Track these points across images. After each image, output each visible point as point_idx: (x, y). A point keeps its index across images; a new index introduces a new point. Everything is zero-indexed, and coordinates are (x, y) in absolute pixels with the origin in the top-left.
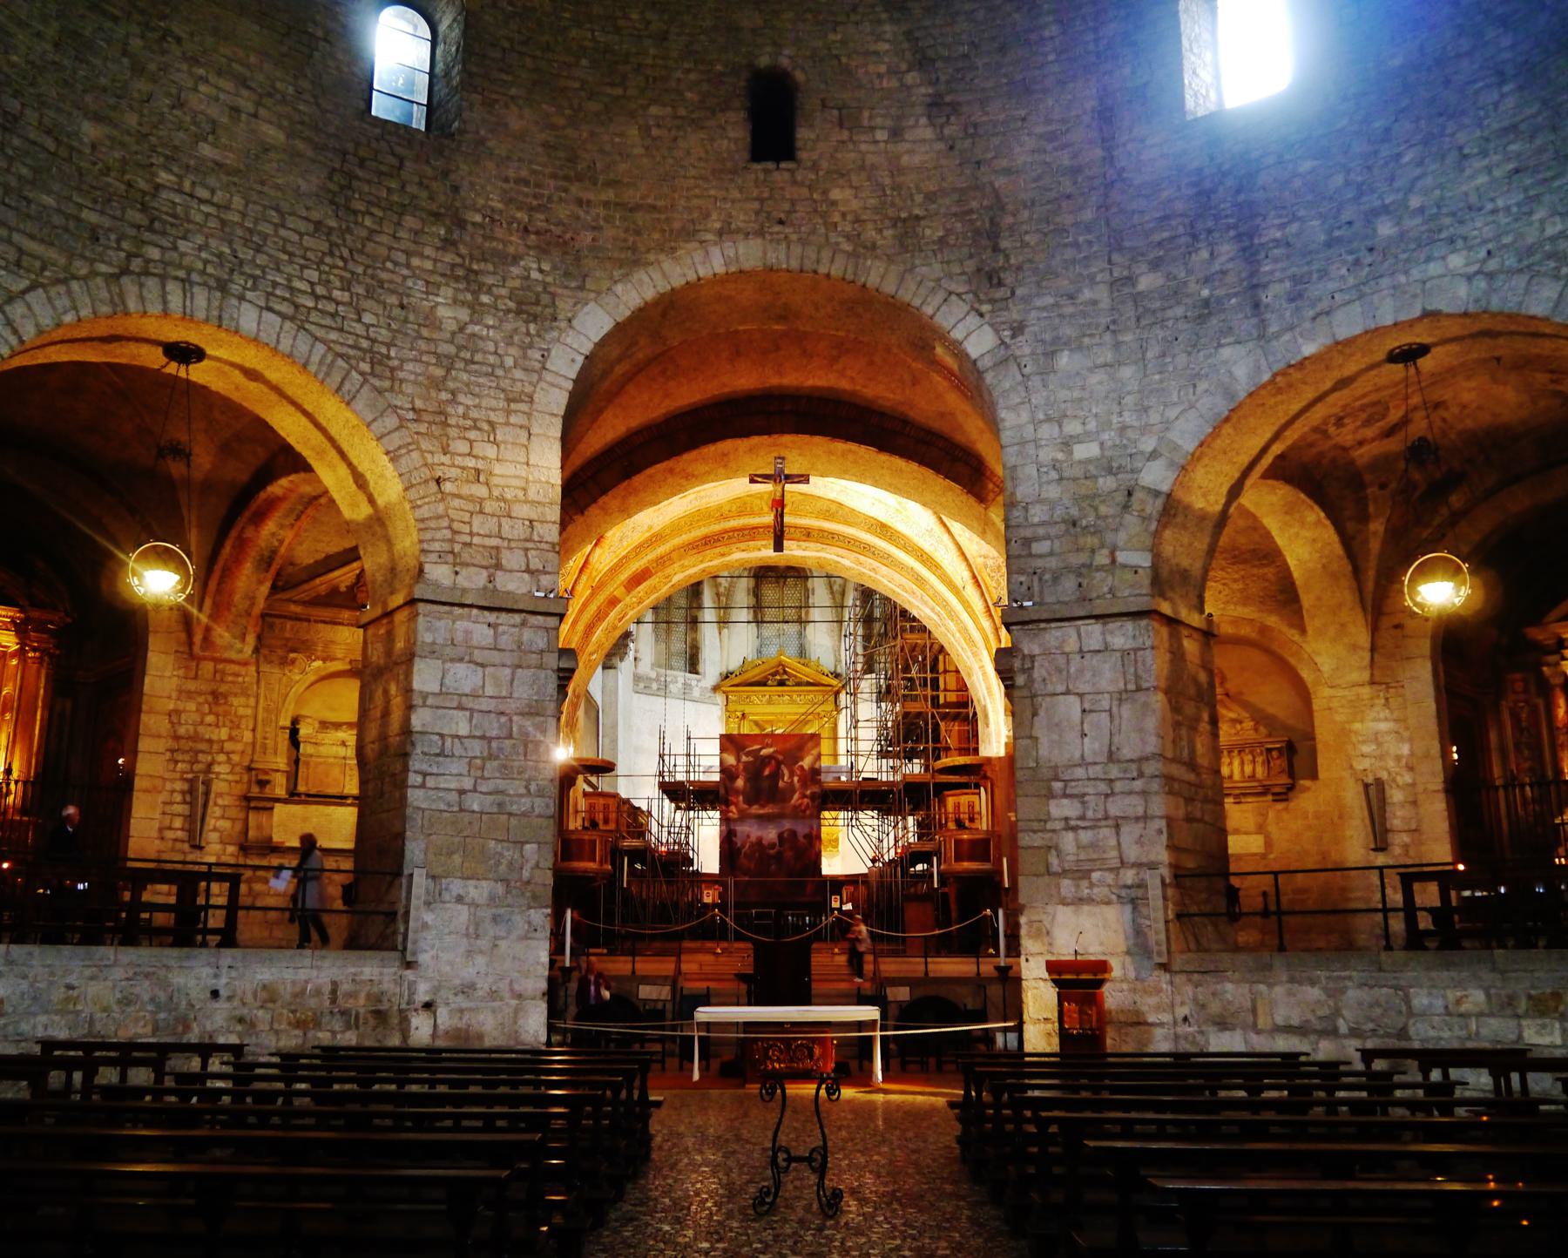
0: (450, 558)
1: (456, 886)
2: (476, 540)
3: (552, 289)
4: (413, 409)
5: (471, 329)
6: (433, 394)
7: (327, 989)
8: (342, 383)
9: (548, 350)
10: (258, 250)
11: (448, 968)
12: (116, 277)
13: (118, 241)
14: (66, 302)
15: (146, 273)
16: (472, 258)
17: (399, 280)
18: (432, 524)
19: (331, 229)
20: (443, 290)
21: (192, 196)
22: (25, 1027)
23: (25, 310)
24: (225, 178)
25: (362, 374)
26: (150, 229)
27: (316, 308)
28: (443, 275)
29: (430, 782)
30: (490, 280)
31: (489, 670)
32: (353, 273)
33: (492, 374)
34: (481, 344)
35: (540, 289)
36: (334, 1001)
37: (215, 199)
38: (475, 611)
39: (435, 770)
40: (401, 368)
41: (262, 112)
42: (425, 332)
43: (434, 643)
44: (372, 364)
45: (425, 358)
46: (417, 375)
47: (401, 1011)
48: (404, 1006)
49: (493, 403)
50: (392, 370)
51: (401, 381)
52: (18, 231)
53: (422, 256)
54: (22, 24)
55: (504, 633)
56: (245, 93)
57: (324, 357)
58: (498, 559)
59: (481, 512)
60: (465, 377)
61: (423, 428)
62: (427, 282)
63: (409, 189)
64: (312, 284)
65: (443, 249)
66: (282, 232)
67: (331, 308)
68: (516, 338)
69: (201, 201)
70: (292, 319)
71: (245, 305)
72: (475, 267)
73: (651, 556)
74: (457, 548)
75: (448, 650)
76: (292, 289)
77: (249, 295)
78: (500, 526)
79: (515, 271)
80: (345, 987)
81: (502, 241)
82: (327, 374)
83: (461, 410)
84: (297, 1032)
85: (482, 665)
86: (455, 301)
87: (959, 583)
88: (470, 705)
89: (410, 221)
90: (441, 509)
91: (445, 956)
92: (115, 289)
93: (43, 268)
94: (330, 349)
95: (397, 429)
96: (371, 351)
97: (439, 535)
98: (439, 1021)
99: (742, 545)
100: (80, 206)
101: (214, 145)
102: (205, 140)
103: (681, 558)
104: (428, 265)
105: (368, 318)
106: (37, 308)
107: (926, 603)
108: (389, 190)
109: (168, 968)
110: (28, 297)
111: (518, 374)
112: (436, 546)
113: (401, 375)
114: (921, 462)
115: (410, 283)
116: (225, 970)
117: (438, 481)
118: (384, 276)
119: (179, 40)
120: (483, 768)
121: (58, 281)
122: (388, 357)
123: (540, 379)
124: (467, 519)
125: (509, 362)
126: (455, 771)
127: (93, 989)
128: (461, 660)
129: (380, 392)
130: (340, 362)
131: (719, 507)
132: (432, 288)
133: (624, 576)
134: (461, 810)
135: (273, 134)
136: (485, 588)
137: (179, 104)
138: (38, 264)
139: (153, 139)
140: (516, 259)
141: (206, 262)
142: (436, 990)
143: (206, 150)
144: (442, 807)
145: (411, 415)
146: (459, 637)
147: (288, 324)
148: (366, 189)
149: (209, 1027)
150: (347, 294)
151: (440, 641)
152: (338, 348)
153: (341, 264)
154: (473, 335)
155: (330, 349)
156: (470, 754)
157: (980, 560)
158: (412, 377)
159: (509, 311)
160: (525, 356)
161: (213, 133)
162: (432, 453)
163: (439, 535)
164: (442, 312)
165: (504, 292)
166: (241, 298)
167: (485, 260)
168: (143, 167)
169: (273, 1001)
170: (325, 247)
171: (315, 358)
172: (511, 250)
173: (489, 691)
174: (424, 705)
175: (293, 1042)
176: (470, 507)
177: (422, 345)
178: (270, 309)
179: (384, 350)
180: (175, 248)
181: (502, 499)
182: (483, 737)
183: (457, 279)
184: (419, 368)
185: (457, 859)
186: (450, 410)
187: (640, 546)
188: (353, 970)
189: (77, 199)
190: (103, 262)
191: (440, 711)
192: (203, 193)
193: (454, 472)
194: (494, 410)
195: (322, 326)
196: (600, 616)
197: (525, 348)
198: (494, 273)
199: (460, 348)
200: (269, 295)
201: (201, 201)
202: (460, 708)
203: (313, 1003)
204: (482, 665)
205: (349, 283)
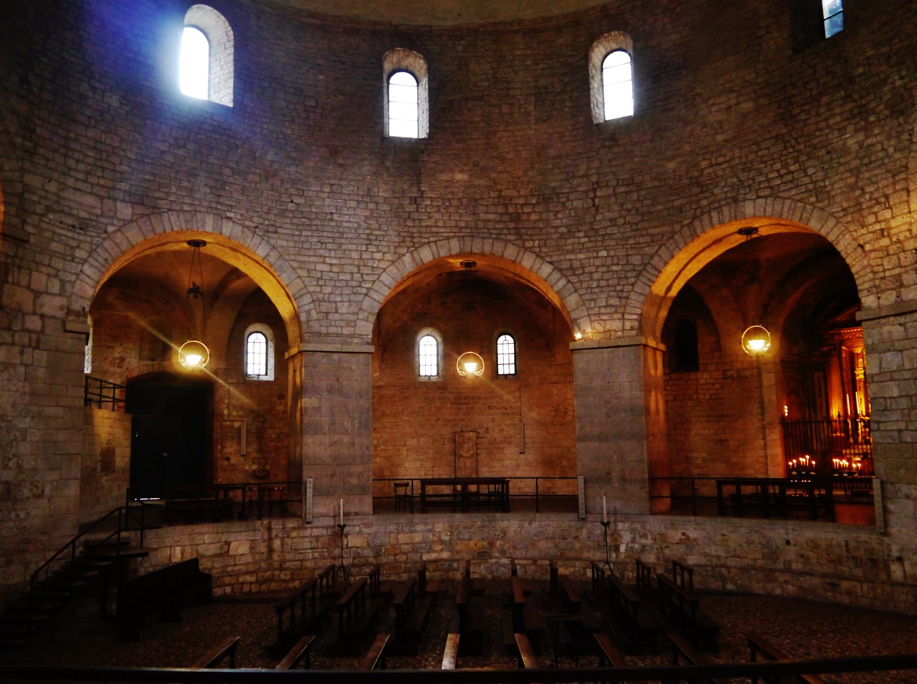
0: (874, 290)
1: (905, 489)
2: (887, 274)
3: (909, 86)
4: (843, 210)
5: (870, 141)
6: (852, 195)
7: (843, 544)
8: (801, 216)
9: (912, 130)
10: (750, 170)
11: (906, 538)
12: (691, 223)
13: (690, 207)
14: (674, 245)
15: (703, 213)
16: (861, 97)
17: (824, 138)
18: (862, 273)
19: (784, 135)
20: (848, 131)
21: (717, 164)
22: (707, 550)
23: (659, 258)
24: (729, 145)
25: (812, 204)
26: (702, 192)
27: (782, 183)
28: (847, 119)
29: (882, 427)
30: (873, 105)
31: (905, 353)
32: (798, 151)
33: (883, 164)
34: (873, 149)
35: (902, 91)
36: (848, 551)
37: (727, 158)
38: (892, 318)
39: (884, 419)
40: (833, 189)
41: (741, 99)
42: (842, 160)
43: (873, 343)
44: (817, 196)
45: (844, 176)
46: (841, 188)
47: (884, 560)
48: (886, 558)
49: (885, 182)
50: (828, 193)
51: (834, 196)
52: (650, 228)
53: (834, 115)
54: (635, 144)
55: (911, 327)
56: (732, 96)
57: (790, 206)
58: (901, 281)
59: (888, 255)
60: (867, 175)
61: (849, 219)
62: (839, 130)
63: (821, 81)
64: (778, 171)
65: (844, 104)
66: (760, 153)
67: (789, 177)
68: (893, 133)
69: (721, 164)
70: (770, 196)
71: (747, 202)
72: (864, 102)
74: (877, 282)
75: (881, 346)
76: (768, 180)
77: (748, 196)
78: (899, 259)
79: (886, 88)
80: (852, 544)
81: (878, 74)
82: (793, 215)
83: (867, 197)
84: (832, 566)
85: (901, 351)
86: (856, 131)
88: (897, 377)
89: (825, 99)
90: (865, 262)
91: (904, 530)
92: (692, 228)
93: (662, 237)
94: (793, 200)
95: (835, 226)
96: (815, 189)
97: (866, 279)
98: (906, 569)
100: (673, 201)
101: (723, 133)
102: (718, 133)
104: (838, 119)
105: (810, 171)
106: (663, 256)
108: (810, 90)
109: (764, 528)
110: (659, 252)
111: (898, 155)
112: (866, 285)
113: (833, 193)
115: (830, 136)
116: (790, 531)
117: (862, 246)
118: (815, 141)
119: (700, 95)
120: (909, 415)
121: (670, 238)
122: (825, 186)
123: (910, 151)
124: (880, 263)
125: (891, 150)
126: (894, 419)
127: (733, 536)
128: (889, 350)
129: (823, 209)
130: (800, 204)
132: (842, 131)
134: (901, 442)
135: (747, 106)
136: (896, 301)
137: (705, 125)
138: (660, 236)
139: (697, 150)
140: (885, 81)
141: (726, 192)
142: (902, 550)
143: (720, 138)
144: (890, 441)
145: (842, 214)
146: (886, 336)
147: (769, 200)
148: (798, 98)
149: (788, 558)
150: (797, 165)
151: (876, 342)
152: (797, 197)
153: (791, 150)
154: (869, 145)
155: (793, 200)
156: (901, 407)
158: (839, 191)
159: (887, 117)
160: (900, 142)
161: (721, 127)
162: (855, 231)
163: (866, 279)
164: (850, 142)
165: (882, 107)
166: (745, 200)
167: (869, 94)
168: (694, 166)
169: (817, 548)
170: (781, 147)
171: (786, 209)
172: (882, 76)
173: (907, 365)
174: (873, 382)
175: (830, 570)
176: (881, 254)
177: (842, 169)
178: (759, 197)
179: (822, 184)
180: (713, 194)
181: (899, 241)
182: (907, 396)
183: (854, 117)
184: (841, 184)
185: (902, 472)
186: (862, 200)
188: (854, 535)
189: (671, 198)
190: (686, 219)
191: (882, 384)
192: (721, 160)
193: (870, 236)
194: (886, 186)
195: (786, 190)
197: (900, 134)
198: (876, 98)
199: (861, 159)
200: (757, 190)
201: (721, 164)
202: (892, 380)
203: (837, 551)
204: (901, 351)
205: (798, 157)
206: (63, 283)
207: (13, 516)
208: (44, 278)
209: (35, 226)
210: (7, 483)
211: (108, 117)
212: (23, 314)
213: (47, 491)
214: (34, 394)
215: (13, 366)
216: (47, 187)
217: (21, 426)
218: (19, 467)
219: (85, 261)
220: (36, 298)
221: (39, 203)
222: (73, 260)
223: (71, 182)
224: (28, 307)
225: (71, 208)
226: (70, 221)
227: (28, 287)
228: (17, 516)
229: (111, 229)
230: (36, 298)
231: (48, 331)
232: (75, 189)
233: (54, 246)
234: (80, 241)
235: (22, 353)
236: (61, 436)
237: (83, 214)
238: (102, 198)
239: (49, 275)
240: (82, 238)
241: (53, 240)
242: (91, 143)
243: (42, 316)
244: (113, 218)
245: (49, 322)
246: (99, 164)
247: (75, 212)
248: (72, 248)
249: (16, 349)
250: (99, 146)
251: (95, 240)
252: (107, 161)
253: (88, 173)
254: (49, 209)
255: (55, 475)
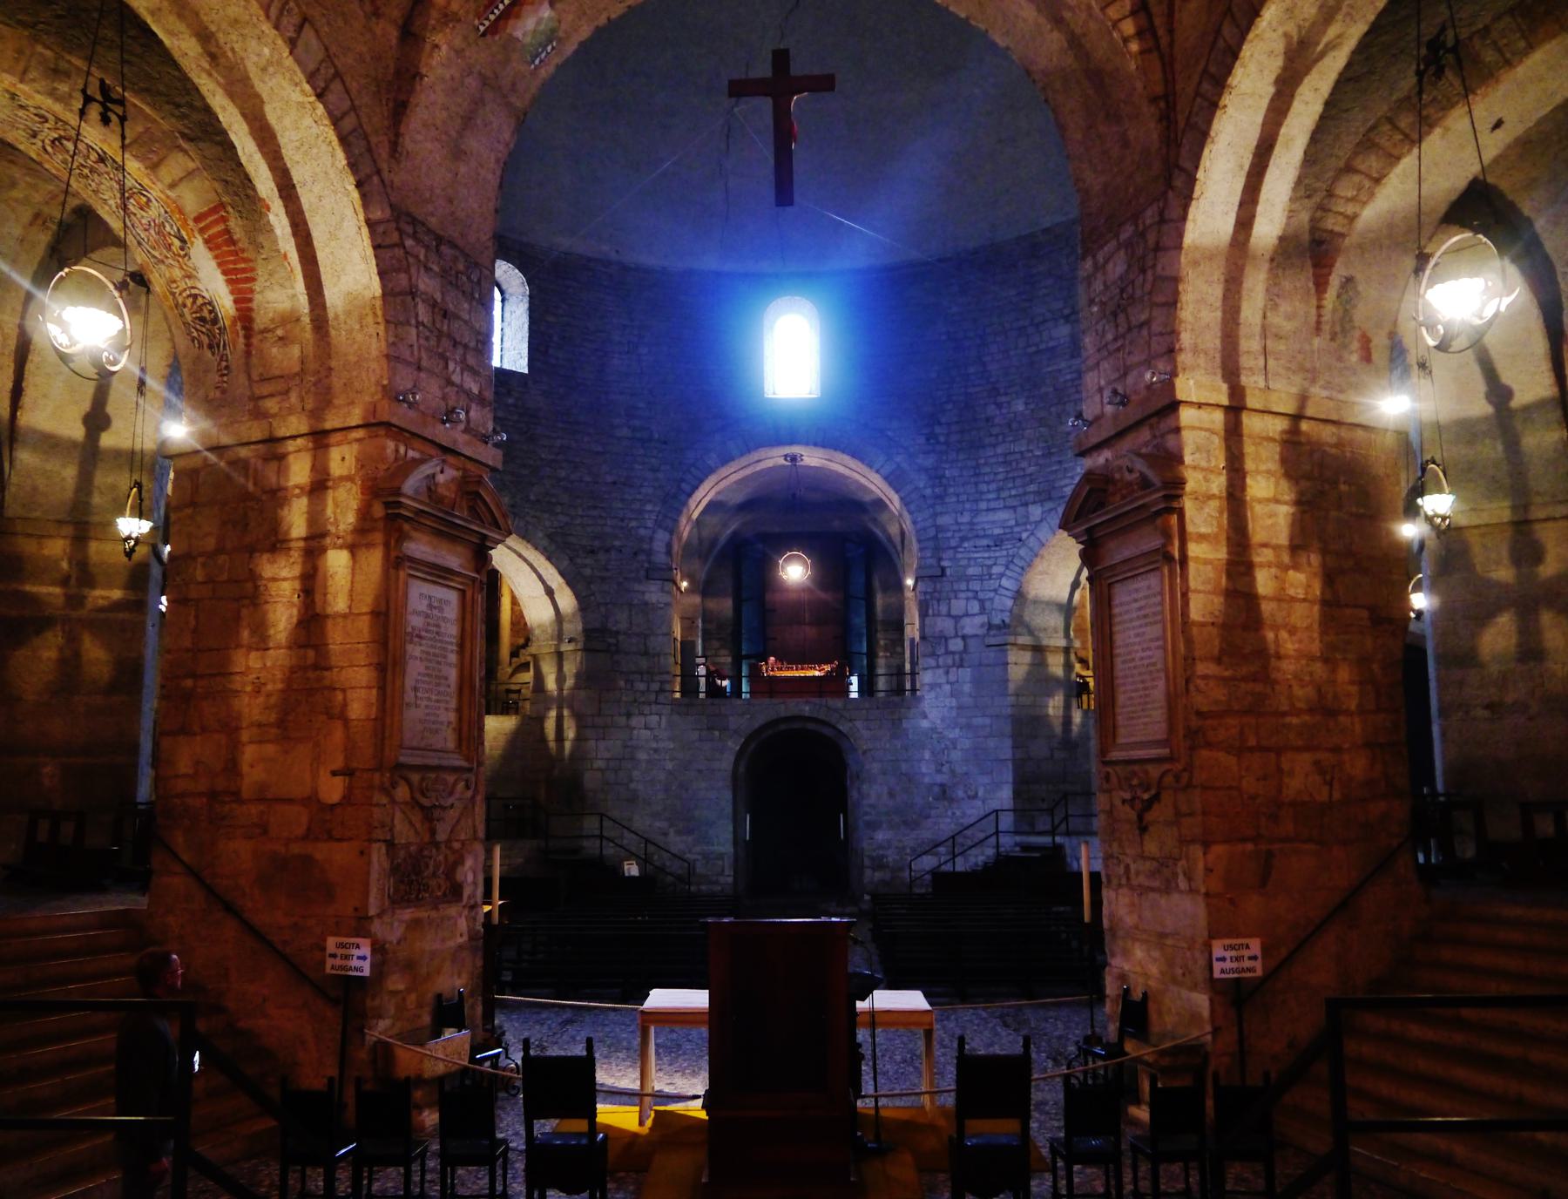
206: (982, 602)
207: (949, 813)
208: (962, 603)
209: (950, 559)
210: (942, 785)
211: (1014, 426)
212: (946, 639)
213: (981, 793)
214: (960, 708)
215: (940, 685)
216: (960, 520)
217: (951, 736)
218: (952, 772)
219: (1002, 575)
220: (956, 623)
221: (953, 537)
222: (990, 579)
223: (983, 505)
224: (950, 631)
225: (984, 530)
226: (985, 542)
227: (949, 615)
228: (954, 814)
229: (1024, 535)
230: (956, 623)
231: (971, 649)
232: (988, 510)
233: (971, 571)
234: (996, 558)
235: (947, 673)
236: (991, 743)
237: (997, 531)
238: (1014, 508)
239: (967, 599)
240: (997, 554)
241: (969, 566)
242: (1001, 460)
243: (964, 638)
244: (1025, 524)
245: (971, 642)
246: (1011, 475)
247: (989, 532)
248: (990, 567)
249: (941, 671)
250: (1009, 458)
251: (1011, 552)
252: (1016, 469)
253: (999, 490)
254: (963, 539)
255: (986, 780)
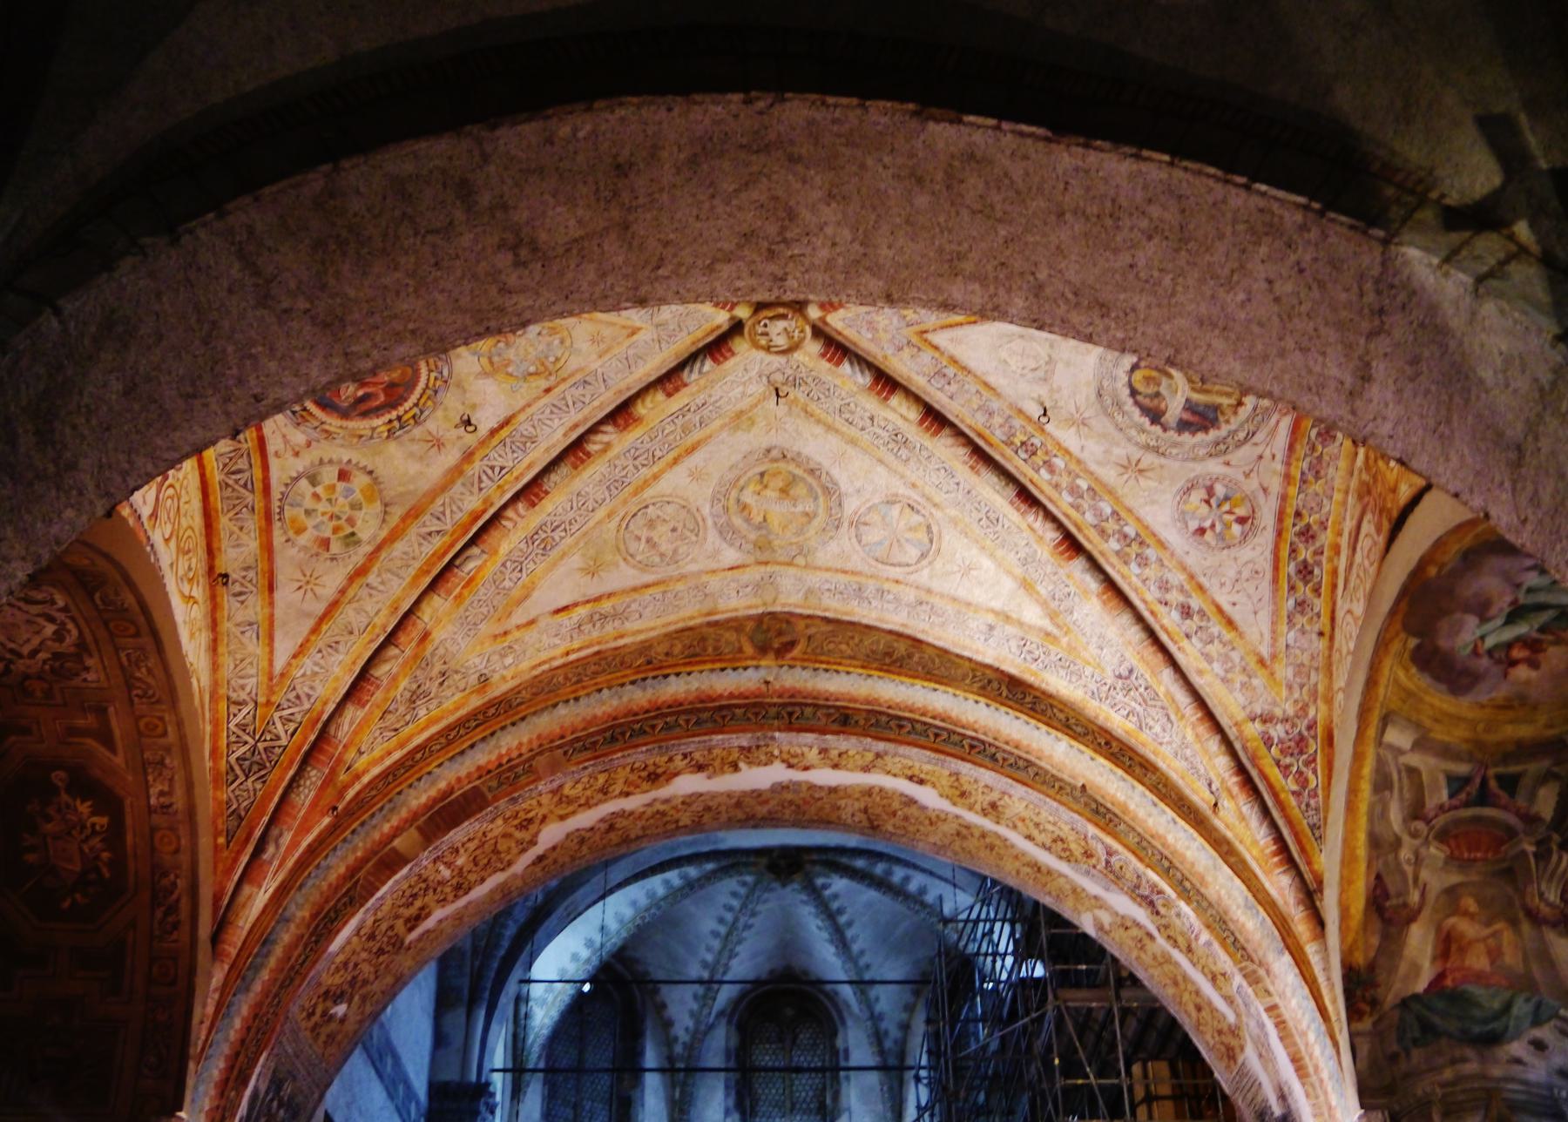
73: (483, 757)
87: (1200, 797)
99: (694, 745)
103: (554, 768)
107: (1114, 875)
114: (1180, 150)
131: (645, 648)
133: (419, 797)
157: (1253, 730)
187: (461, 723)
196: (352, 893)
